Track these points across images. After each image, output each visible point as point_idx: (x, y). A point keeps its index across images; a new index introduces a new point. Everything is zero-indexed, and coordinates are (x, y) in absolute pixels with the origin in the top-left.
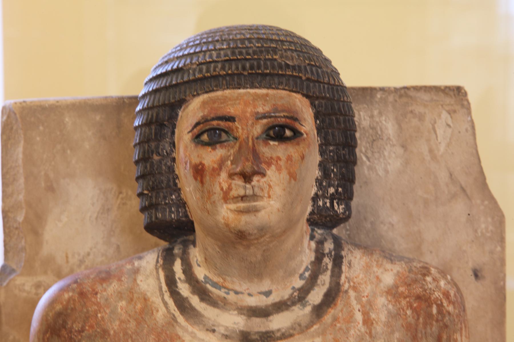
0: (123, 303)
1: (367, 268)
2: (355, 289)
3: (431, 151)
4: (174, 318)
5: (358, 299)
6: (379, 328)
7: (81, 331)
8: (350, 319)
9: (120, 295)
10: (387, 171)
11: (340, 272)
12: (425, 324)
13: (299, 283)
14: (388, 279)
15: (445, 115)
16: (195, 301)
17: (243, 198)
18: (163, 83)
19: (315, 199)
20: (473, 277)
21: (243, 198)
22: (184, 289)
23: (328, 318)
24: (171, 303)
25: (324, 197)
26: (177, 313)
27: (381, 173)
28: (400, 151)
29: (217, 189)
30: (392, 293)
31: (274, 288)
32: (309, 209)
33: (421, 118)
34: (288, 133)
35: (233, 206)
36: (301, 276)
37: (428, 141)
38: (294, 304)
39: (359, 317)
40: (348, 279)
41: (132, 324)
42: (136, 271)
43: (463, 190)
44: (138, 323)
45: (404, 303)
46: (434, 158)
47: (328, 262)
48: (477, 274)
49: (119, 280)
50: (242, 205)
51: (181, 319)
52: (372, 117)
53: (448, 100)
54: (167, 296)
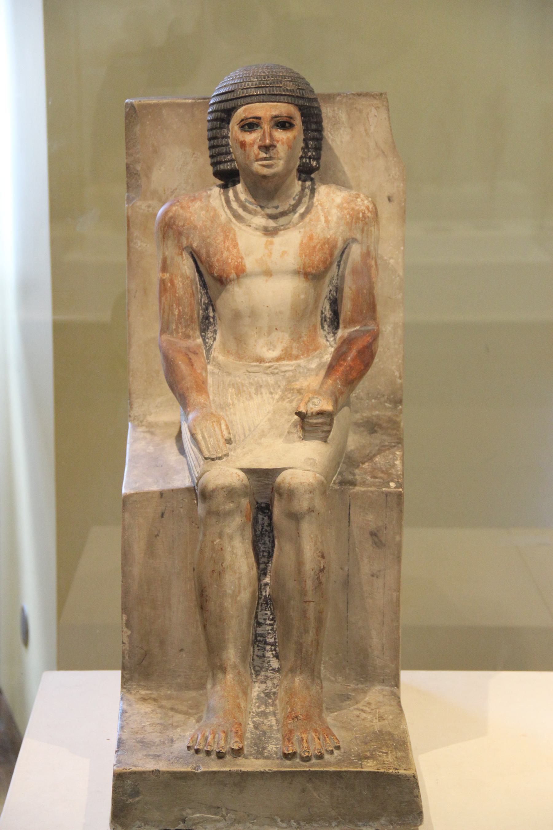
0: (204, 212)
1: (328, 194)
2: (321, 205)
3: (366, 130)
4: (231, 221)
5: (323, 210)
6: (332, 224)
7: (184, 226)
8: (318, 219)
9: (202, 209)
10: (342, 142)
11: (314, 196)
12: (356, 223)
13: (293, 202)
14: (338, 200)
15: (373, 110)
16: (240, 211)
17: (265, 159)
18: (223, 97)
19: (301, 158)
20: (387, 201)
21: (265, 159)
22: (235, 205)
23: (307, 219)
24: (228, 212)
25: (306, 157)
26: (232, 217)
27: (339, 143)
28: (349, 130)
29: (252, 154)
30: (340, 207)
31: (280, 204)
32: (298, 163)
33: (361, 111)
34: (287, 125)
35: (260, 163)
36: (294, 199)
37: (364, 125)
38: (290, 212)
39: (323, 219)
40: (318, 200)
41: (209, 223)
42: (209, 196)
43: (383, 152)
44: (212, 222)
45: (345, 212)
46: (367, 134)
47: (307, 191)
48: (390, 199)
49: (201, 200)
50: (265, 163)
51: (233, 220)
52: (334, 111)
53: (375, 102)
54: (226, 208)
